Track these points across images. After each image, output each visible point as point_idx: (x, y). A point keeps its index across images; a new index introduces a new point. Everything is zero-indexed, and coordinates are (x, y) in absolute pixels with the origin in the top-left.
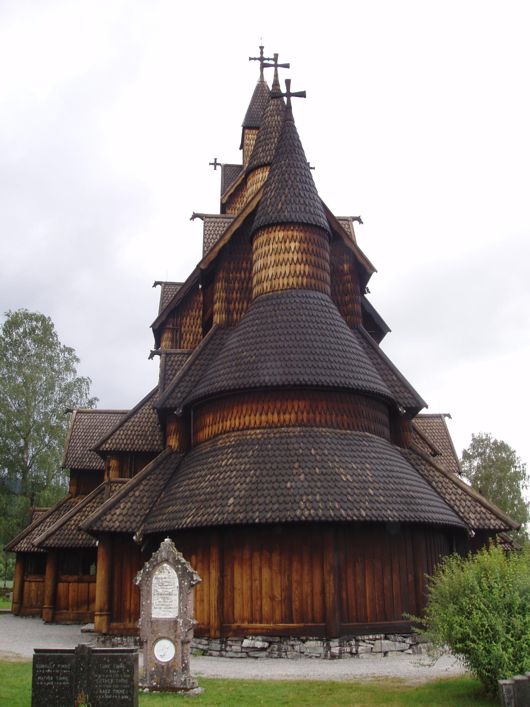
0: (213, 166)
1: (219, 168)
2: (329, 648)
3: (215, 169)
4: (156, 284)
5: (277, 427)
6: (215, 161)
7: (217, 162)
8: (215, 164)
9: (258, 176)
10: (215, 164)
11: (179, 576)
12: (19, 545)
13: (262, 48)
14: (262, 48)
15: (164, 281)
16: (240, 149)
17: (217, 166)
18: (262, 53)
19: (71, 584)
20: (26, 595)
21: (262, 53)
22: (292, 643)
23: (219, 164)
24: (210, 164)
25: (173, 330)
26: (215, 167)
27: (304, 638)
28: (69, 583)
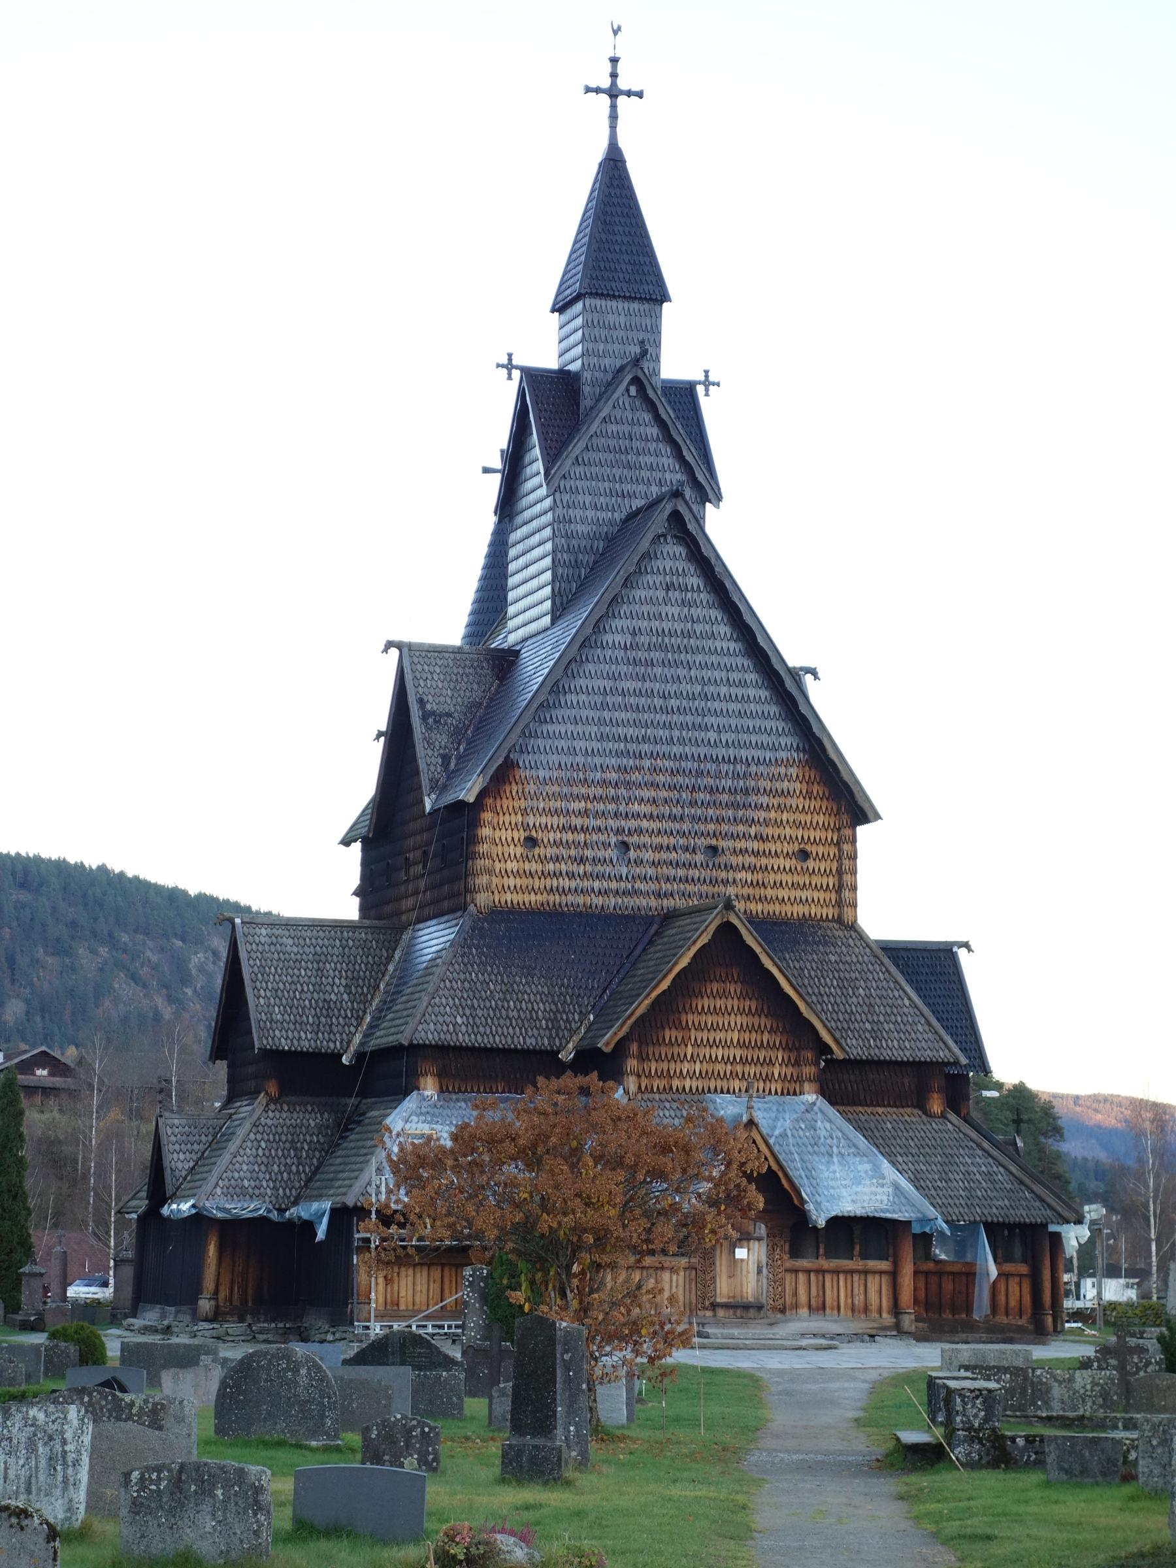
0: (505, 371)
1: (516, 374)
3: (510, 378)
4: (389, 645)
6: (510, 360)
7: (515, 362)
8: (509, 366)
10: (509, 366)
13: (614, 61)
14: (614, 61)
15: (406, 638)
16: (553, 311)
17: (514, 371)
18: (614, 75)
21: (614, 75)
23: (517, 367)
24: (498, 366)
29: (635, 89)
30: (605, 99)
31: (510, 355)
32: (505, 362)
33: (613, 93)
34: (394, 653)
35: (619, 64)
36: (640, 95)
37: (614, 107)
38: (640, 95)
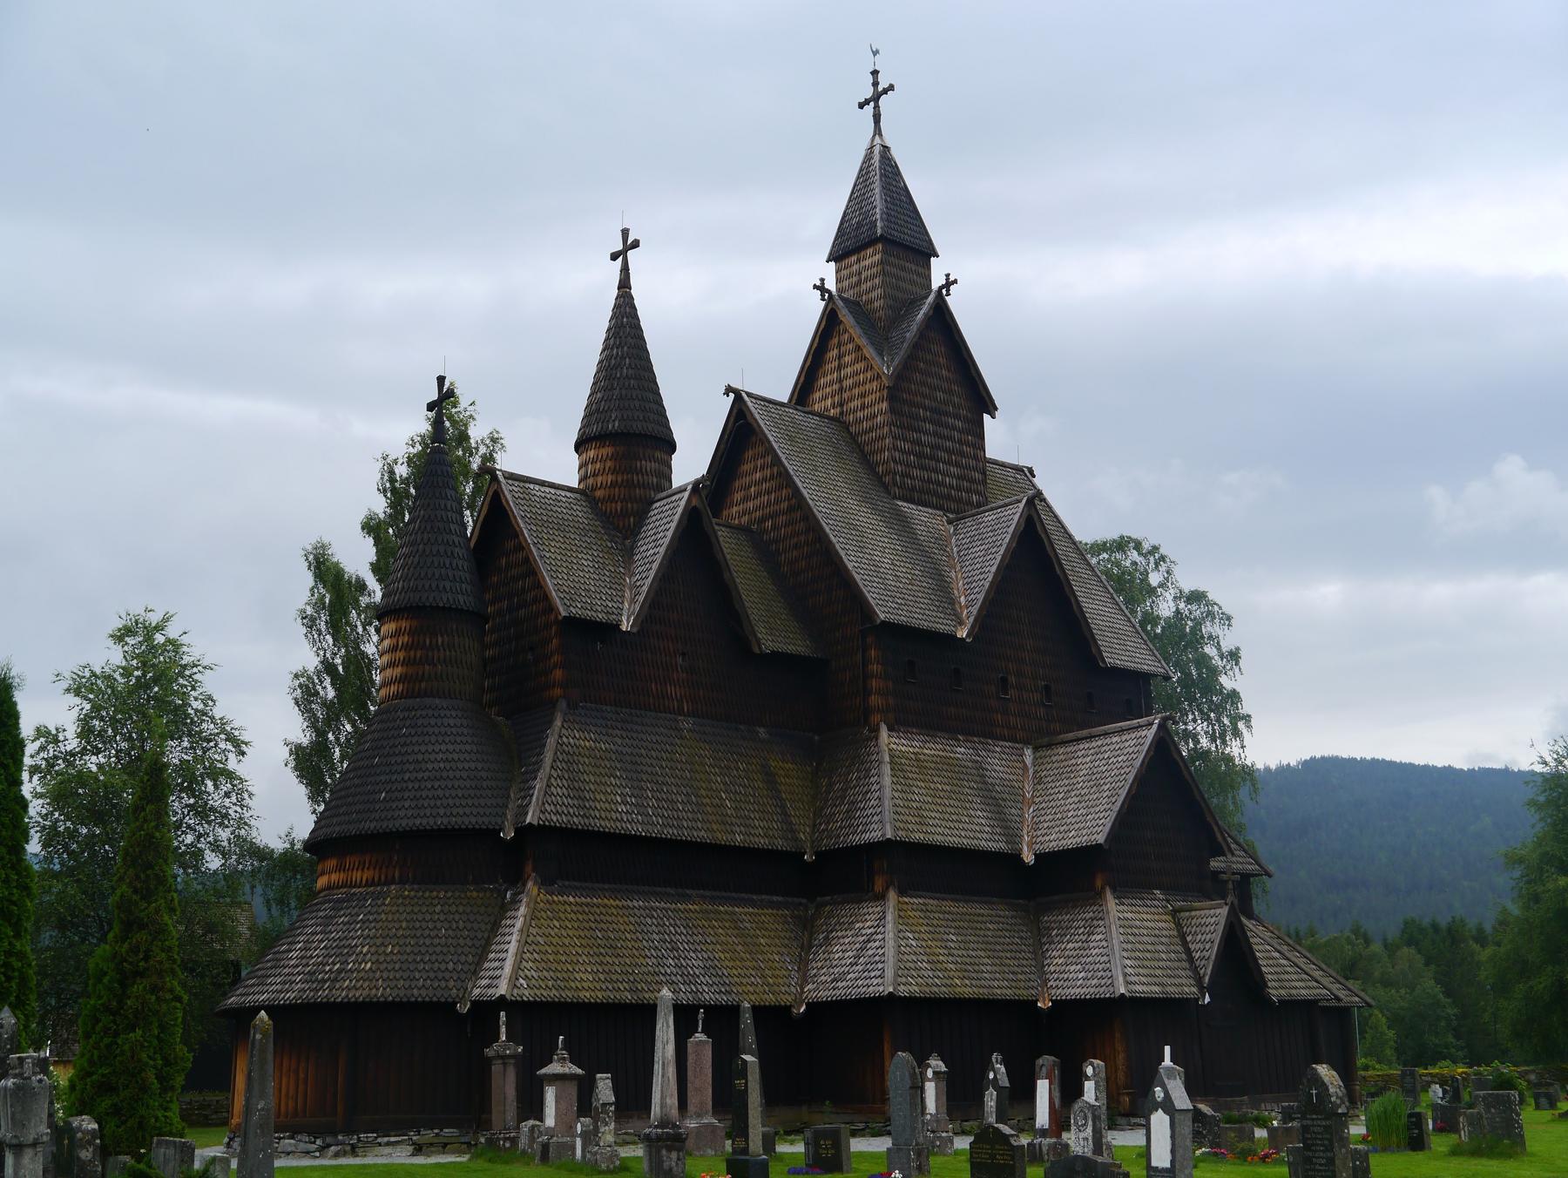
3: (823, 299)
7: (826, 286)
8: (821, 288)
24: (815, 287)
26: (823, 296)
31: (822, 280)
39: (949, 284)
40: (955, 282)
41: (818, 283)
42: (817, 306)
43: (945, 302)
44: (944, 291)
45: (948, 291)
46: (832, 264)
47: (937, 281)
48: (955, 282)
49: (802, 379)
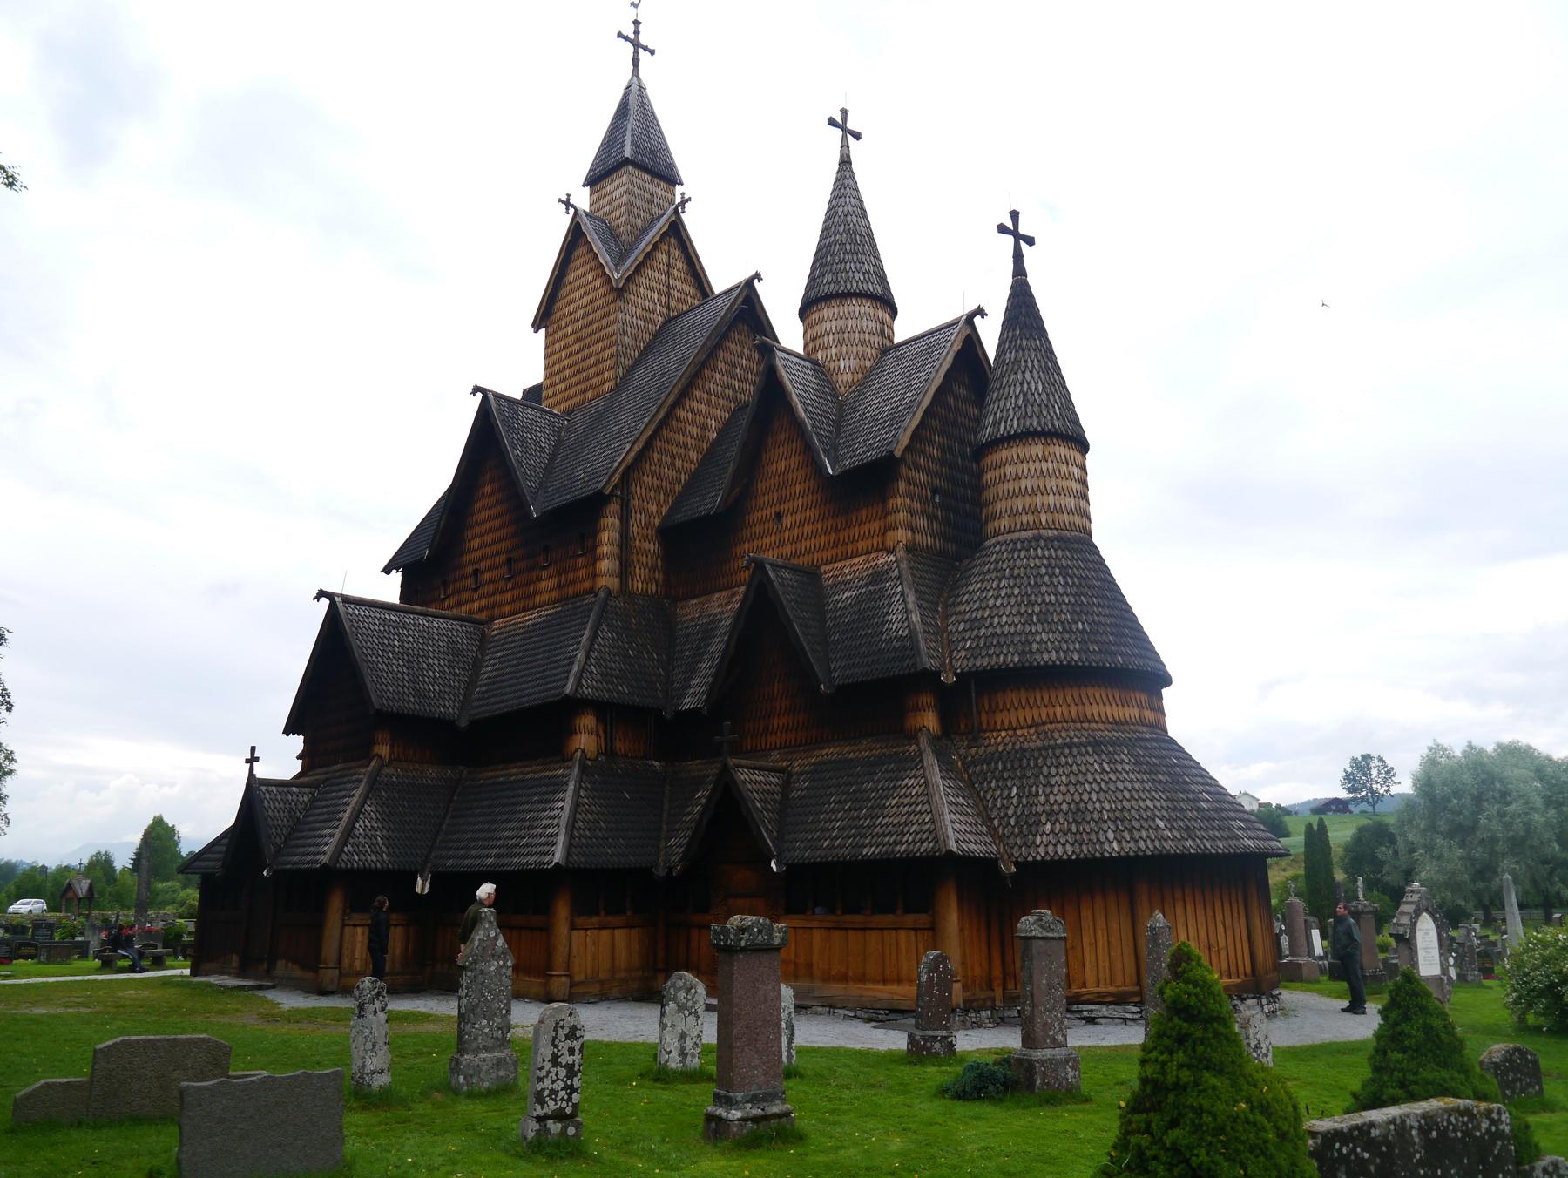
0: (564, 206)
1: (572, 211)
2: (1262, 1006)
4: (476, 389)
5: (1122, 724)
7: (572, 202)
8: (568, 204)
9: (851, 308)
11: (1438, 927)
12: (344, 857)
13: (637, 23)
14: (637, 23)
18: (637, 32)
19: (589, 933)
20: (346, 952)
21: (637, 32)
22: (1236, 1002)
23: (573, 206)
24: (560, 201)
25: (622, 499)
26: (567, 209)
27: (1245, 996)
28: (587, 929)
29: (650, 47)
30: (629, 48)
31: (568, 195)
32: (564, 198)
33: (636, 45)
34: (479, 395)
35: (641, 26)
36: (652, 52)
37: (636, 53)
38: (652, 52)
39: (685, 201)
40: (689, 199)
41: (564, 198)
42: (563, 222)
43: (679, 218)
44: (680, 209)
45: (683, 208)
46: (587, 189)
47: (678, 200)
48: (689, 199)
49: (551, 287)
